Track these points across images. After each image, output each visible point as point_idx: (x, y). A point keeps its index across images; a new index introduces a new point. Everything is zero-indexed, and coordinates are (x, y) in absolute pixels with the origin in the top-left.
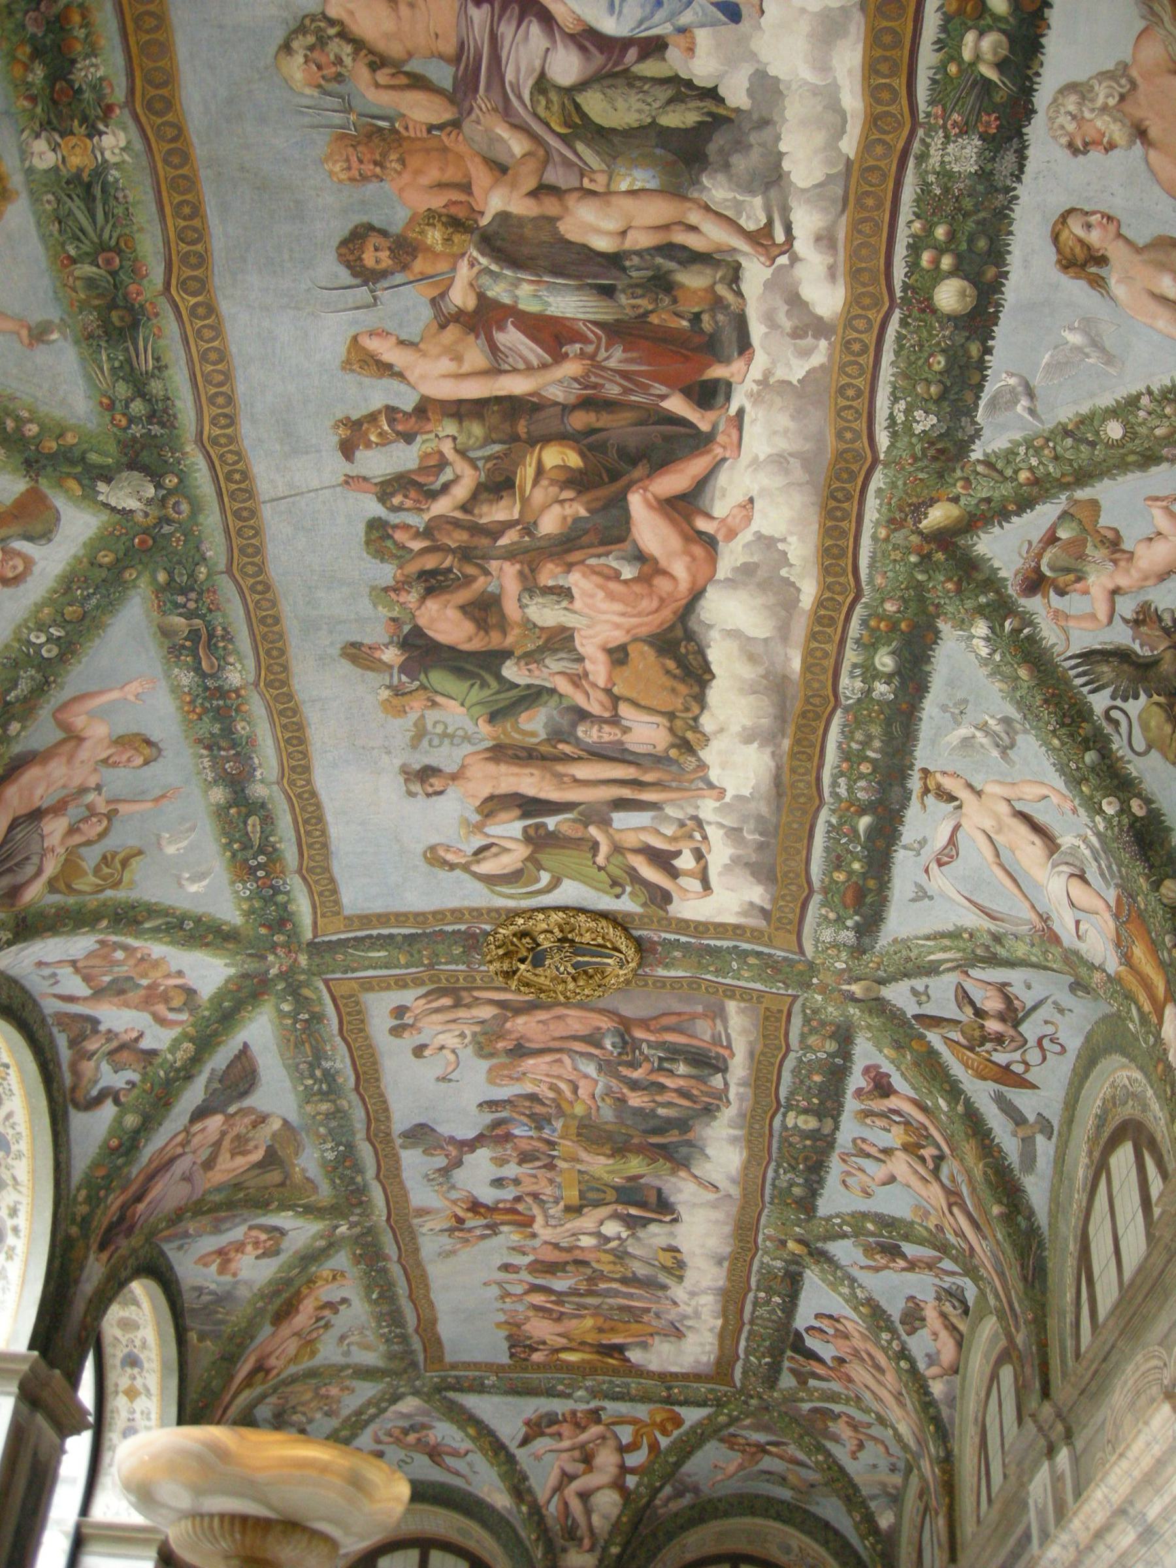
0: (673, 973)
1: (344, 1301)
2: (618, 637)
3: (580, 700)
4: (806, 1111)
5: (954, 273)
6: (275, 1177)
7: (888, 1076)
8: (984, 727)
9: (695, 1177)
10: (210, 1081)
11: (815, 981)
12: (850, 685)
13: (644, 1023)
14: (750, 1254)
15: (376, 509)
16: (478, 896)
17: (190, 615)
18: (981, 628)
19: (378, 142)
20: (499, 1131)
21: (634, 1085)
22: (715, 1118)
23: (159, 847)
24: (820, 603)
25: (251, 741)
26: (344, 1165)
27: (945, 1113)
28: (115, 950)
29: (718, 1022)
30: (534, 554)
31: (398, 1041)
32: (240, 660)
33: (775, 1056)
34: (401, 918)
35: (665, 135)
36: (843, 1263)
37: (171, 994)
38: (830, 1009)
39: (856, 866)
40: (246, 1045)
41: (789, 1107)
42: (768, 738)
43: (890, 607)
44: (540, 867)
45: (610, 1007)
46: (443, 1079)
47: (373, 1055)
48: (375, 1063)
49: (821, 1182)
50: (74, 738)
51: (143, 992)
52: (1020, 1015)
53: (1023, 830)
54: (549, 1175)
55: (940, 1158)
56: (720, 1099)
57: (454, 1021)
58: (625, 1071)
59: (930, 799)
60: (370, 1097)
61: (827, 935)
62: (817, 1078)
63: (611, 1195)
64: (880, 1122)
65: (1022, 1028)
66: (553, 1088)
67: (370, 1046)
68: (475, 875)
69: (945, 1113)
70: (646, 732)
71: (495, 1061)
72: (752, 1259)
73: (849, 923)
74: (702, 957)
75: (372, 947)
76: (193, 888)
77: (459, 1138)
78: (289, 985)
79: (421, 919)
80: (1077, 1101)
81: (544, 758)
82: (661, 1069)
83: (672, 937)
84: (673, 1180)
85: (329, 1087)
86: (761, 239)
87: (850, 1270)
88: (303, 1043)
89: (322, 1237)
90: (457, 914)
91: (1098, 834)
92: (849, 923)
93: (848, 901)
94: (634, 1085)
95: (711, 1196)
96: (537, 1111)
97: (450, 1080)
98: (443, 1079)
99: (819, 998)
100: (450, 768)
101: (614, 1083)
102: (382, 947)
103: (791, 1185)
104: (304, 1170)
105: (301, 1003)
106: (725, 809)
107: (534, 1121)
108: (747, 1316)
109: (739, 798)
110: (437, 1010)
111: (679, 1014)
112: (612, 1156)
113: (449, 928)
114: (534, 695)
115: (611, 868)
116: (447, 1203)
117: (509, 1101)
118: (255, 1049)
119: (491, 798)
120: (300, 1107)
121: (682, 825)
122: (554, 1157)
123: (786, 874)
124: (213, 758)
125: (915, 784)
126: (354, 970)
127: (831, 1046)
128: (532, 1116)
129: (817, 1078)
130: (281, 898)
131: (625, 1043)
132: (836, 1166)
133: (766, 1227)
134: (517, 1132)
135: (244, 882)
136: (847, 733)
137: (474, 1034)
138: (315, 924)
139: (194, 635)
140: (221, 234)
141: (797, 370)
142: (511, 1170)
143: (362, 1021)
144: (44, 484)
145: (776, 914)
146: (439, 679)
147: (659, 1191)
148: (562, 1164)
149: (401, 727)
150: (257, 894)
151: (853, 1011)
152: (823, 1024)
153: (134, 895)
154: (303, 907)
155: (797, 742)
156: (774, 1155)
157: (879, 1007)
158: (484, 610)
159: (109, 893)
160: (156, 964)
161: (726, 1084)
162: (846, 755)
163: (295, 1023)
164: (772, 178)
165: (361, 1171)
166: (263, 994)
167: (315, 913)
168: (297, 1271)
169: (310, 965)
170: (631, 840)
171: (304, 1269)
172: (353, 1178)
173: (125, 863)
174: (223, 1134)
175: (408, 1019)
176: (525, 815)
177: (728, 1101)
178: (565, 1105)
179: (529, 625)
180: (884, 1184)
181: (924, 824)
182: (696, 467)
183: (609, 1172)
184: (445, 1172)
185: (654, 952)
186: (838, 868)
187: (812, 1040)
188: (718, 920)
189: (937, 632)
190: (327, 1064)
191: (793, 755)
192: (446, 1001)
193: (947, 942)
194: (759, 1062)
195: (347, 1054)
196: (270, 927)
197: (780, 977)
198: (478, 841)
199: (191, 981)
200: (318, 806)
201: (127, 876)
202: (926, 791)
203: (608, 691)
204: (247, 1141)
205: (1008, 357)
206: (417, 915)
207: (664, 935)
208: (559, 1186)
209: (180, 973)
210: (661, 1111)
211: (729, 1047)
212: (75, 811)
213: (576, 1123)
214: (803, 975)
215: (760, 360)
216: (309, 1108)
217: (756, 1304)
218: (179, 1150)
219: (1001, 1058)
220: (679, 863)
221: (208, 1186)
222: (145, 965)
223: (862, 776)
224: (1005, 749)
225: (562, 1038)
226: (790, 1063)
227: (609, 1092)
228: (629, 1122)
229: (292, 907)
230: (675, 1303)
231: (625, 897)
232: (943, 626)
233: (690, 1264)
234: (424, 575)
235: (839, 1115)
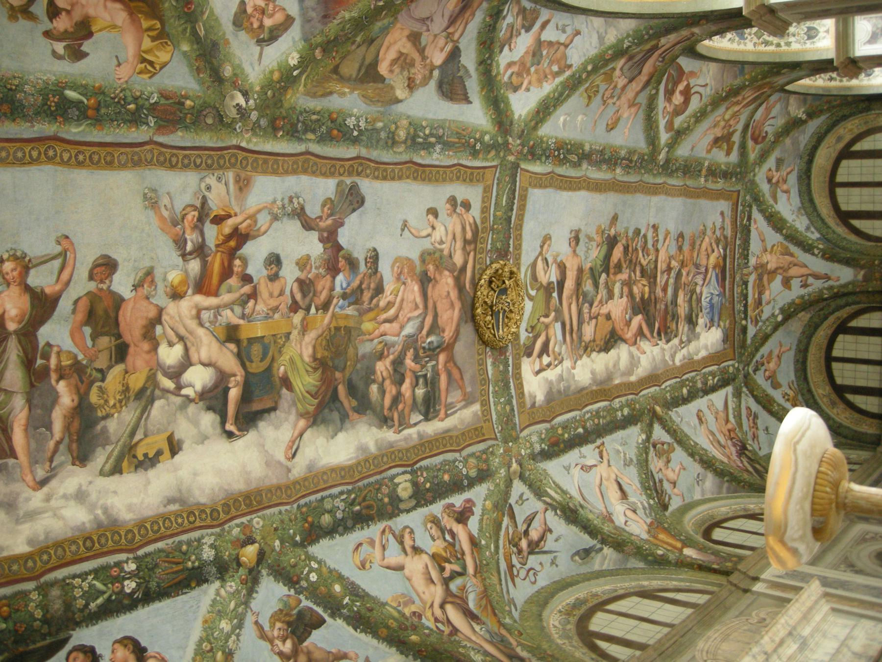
0: (490, 368)
1: (78, 55)
2: (613, 316)
3: (596, 304)
4: (415, 484)
5: (688, 391)
6: (350, 68)
7: (473, 514)
8: (625, 454)
9: (301, 435)
10: (467, 71)
11: (510, 444)
12: (616, 403)
13: (451, 359)
14: (209, 522)
15: (643, 232)
16: (526, 259)
17: (636, 162)
18: (644, 436)
19: (693, 245)
20: (342, 263)
21: (398, 363)
22: (380, 427)
23: (584, 114)
24: (632, 383)
25: (600, 169)
26: (335, 129)
27: (490, 552)
28: (559, 68)
29: (463, 403)
30: (628, 284)
31: (444, 200)
32: (623, 175)
33: (451, 445)
34: (521, 217)
35: (691, 314)
36: (253, 604)
37: (520, 79)
38: (497, 460)
39: (566, 436)
40: (471, 103)
41: (411, 473)
42: (594, 380)
43: (637, 406)
44: (538, 290)
45: (461, 336)
46: (405, 225)
47: (437, 181)
48: (430, 180)
49: (348, 529)
50: (632, 105)
51: (528, 65)
52: (537, 550)
53: (616, 487)
54: (283, 308)
55: (454, 575)
56: (400, 425)
57: (454, 238)
58: (410, 354)
59: (597, 450)
60: (401, 170)
61: (534, 438)
62: (446, 477)
63: (256, 367)
64: (434, 531)
65: (531, 557)
66: (390, 305)
67: (444, 180)
68: (537, 258)
69: (490, 552)
70: (588, 331)
71: (418, 263)
72: (201, 528)
73: (543, 446)
74: (502, 381)
75: (508, 198)
76: (562, 119)
77: (340, 231)
78: (499, 145)
79: (519, 227)
80: (589, 580)
81: (578, 290)
82: (417, 378)
83: (510, 362)
84: (292, 417)
85: (414, 142)
86: (681, 342)
87: (249, 614)
88: (459, 138)
89: (235, 75)
90: (518, 247)
91: (649, 504)
92: (543, 446)
93: (552, 440)
94: (398, 363)
95: (280, 455)
96: (366, 293)
97: (403, 230)
98: (405, 225)
99: (501, 451)
100: (578, 249)
101: (398, 348)
102: (507, 203)
103: (329, 512)
104: (343, 94)
105: (488, 148)
106: (569, 372)
107: (353, 292)
108: (60, 574)
109: (574, 376)
110: (464, 229)
111: (462, 378)
112: (315, 359)
113: (511, 242)
114: (596, 285)
115: (539, 325)
116: (251, 211)
117: (376, 271)
118: (465, 107)
119: (565, 267)
120: (408, 117)
121: (559, 354)
122: (308, 309)
123: (552, 407)
124: (598, 151)
125: (599, 442)
126: (498, 184)
127: (473, 473)
128: (360, 289)
129: (446, 477)
130: (544, 158)
131: (434, 350)
132: (374, 530)
133: (263, 518)
134: (340, 278)
135: (555, 143)
136: (604, 409)
137: (442, 251)
138: (527, 171)
139: (631, 161)
140: (689, 201)
141: (667, 358)
142: (290, 273)
143: (464, 180)
144: (673, 133)
145: (534, 410)
146: (605, 248)
147: (274, 409)
148: (297, 318)
149: (592, 231)
150: (548, 148)
151: (503, 471)
152: (486, 461)
153: (577, 93)
154: (537, 168)
155: (596, 391)
156: (360, 484)
157: (509, 483)
158: (619, 268)
159: (587, 85)
160: (540, 82)
161: (415, 424)
162: (598, 412)
163: (475, 139)
164: (689, 341)
165: (321, 140)
166: (499, 128)
167: (533, 173)
168: (202, 33)
169: (508, 161)
170: (551, 332)
171: (196, 38)
172: (314, 131)
173: (589, 97)
174: (424, 58)
175: (459, 209)
176: (558, 283)
177: (400, 431)
178: (371, 315)
179: (614, 283)
180: (388, 568)
181: (589, 453)
182: (648, 335)
183: (292, 360)
184: (300, 214)
185: (501, 355)
186: (563, 428)
187: (472, 461)
188: (525, 383)
189: (636, 424)
190: (438, 148)
191: (591, 392)
192: (469, 235)
193: (559, 491)
194: (444, 438)
195: (442, 164)
196: (532, 147)
197: (504, 426)
198: (550, 260)
199: (521, 92)
200: (575, 190)
201: (585, 95)
202: (598, 447)
203: (598, 314)
204: (403, 69)
205: (682, 409)
206: (521, 226)
207: (510, 358)
208: (267, 317)
209: (528, 90)
210: (374, 388)
211: (447, 416)
212: (618, 91)
213: (351, 324)
214: (510, 435)
215: (666, 347)
216: (404, 123)
217: (96, 572)
218: (451, 30)
219: (515, 561)
220: (545, 356)
221: (398, 25)
222: (542, 76)
223: (593, 421)
224: (625, 465)
225: (435, 308)
226: (449, 456)
227: (387, 346)
228: (359, 366)
229: (538, 162)
230: (43, 483)
231: (527, 334)
232: (639, 424)
233: (152, 473)
234: (628, 245)
235: (422, 506)
